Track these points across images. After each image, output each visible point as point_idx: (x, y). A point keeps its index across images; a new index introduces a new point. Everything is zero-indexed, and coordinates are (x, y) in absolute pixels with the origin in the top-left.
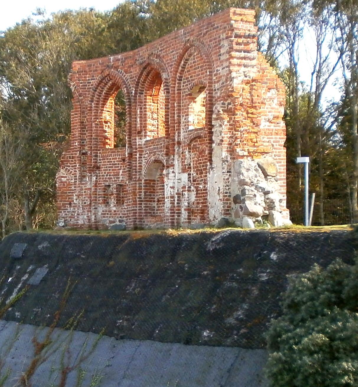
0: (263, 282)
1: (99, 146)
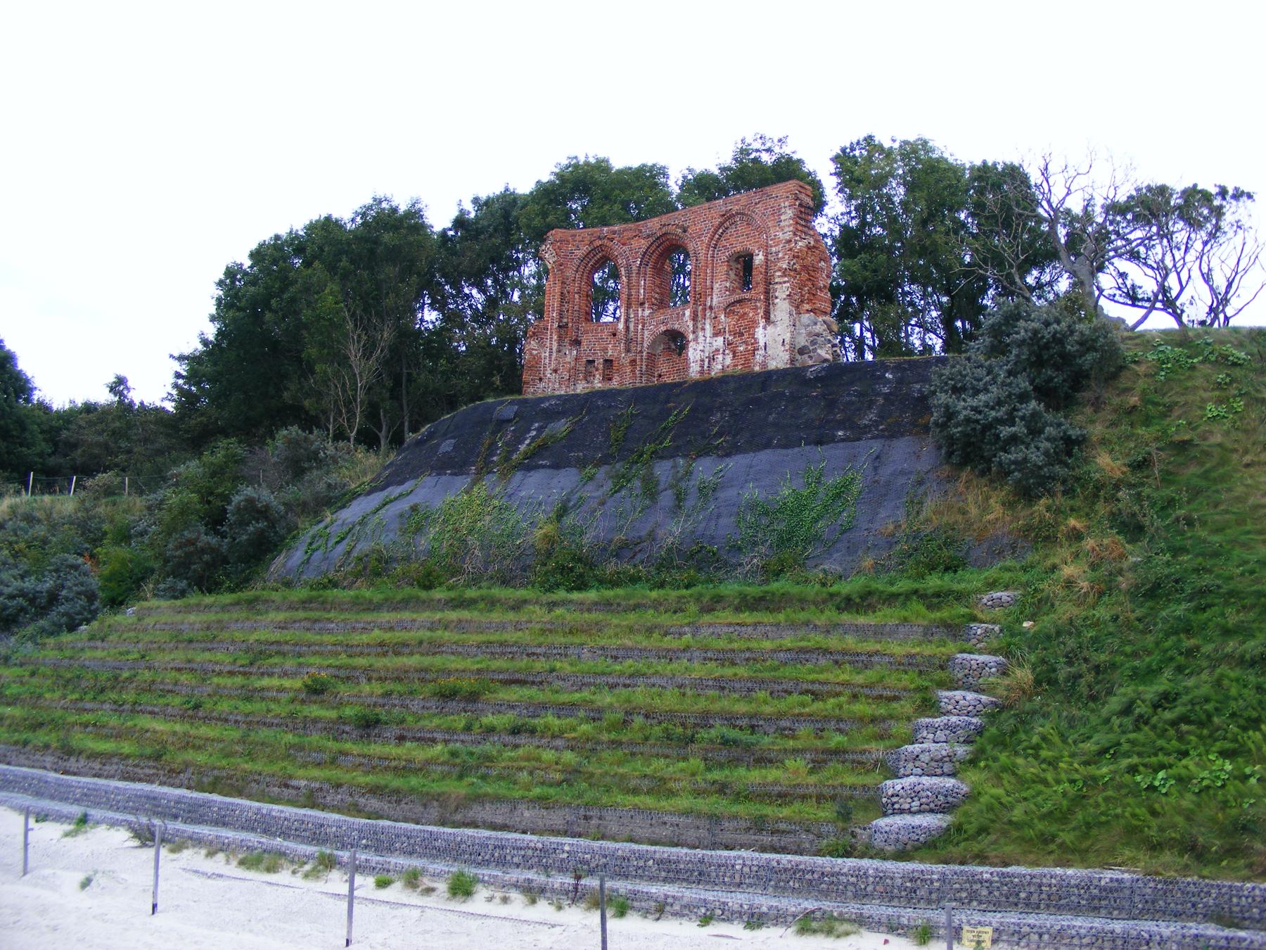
0: (886, 394)
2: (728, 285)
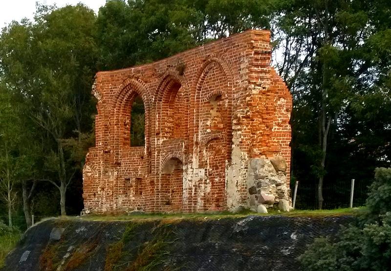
0: (285, 256)
1: (120, 146)
2: (209, 123)
